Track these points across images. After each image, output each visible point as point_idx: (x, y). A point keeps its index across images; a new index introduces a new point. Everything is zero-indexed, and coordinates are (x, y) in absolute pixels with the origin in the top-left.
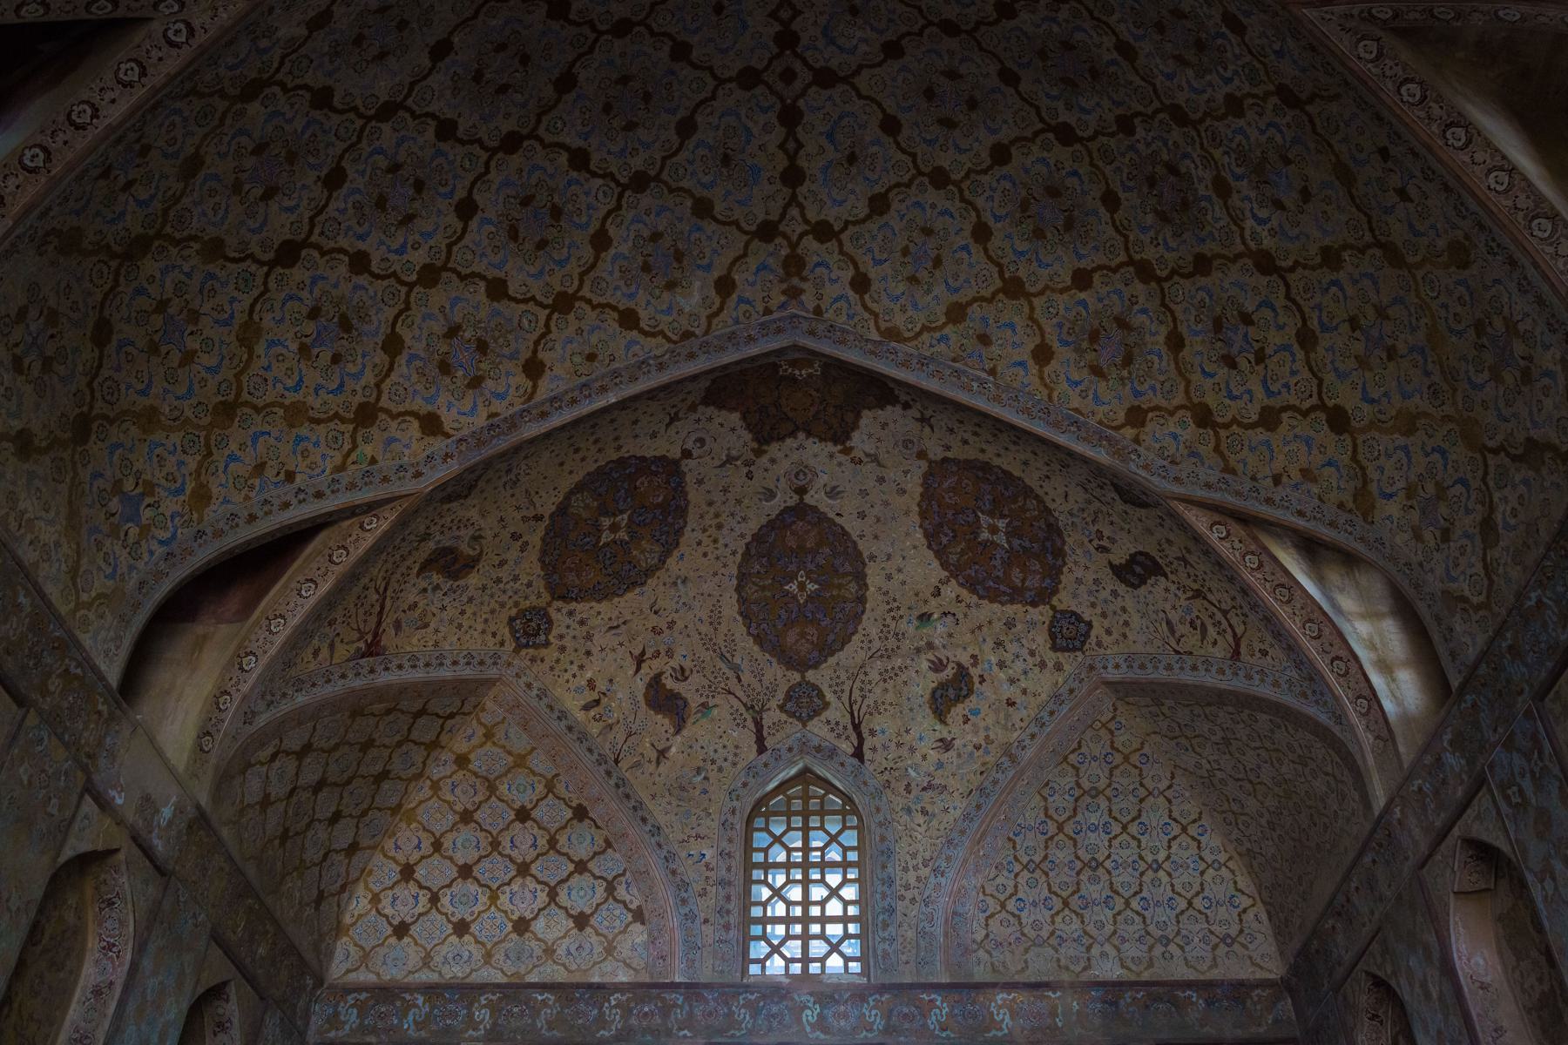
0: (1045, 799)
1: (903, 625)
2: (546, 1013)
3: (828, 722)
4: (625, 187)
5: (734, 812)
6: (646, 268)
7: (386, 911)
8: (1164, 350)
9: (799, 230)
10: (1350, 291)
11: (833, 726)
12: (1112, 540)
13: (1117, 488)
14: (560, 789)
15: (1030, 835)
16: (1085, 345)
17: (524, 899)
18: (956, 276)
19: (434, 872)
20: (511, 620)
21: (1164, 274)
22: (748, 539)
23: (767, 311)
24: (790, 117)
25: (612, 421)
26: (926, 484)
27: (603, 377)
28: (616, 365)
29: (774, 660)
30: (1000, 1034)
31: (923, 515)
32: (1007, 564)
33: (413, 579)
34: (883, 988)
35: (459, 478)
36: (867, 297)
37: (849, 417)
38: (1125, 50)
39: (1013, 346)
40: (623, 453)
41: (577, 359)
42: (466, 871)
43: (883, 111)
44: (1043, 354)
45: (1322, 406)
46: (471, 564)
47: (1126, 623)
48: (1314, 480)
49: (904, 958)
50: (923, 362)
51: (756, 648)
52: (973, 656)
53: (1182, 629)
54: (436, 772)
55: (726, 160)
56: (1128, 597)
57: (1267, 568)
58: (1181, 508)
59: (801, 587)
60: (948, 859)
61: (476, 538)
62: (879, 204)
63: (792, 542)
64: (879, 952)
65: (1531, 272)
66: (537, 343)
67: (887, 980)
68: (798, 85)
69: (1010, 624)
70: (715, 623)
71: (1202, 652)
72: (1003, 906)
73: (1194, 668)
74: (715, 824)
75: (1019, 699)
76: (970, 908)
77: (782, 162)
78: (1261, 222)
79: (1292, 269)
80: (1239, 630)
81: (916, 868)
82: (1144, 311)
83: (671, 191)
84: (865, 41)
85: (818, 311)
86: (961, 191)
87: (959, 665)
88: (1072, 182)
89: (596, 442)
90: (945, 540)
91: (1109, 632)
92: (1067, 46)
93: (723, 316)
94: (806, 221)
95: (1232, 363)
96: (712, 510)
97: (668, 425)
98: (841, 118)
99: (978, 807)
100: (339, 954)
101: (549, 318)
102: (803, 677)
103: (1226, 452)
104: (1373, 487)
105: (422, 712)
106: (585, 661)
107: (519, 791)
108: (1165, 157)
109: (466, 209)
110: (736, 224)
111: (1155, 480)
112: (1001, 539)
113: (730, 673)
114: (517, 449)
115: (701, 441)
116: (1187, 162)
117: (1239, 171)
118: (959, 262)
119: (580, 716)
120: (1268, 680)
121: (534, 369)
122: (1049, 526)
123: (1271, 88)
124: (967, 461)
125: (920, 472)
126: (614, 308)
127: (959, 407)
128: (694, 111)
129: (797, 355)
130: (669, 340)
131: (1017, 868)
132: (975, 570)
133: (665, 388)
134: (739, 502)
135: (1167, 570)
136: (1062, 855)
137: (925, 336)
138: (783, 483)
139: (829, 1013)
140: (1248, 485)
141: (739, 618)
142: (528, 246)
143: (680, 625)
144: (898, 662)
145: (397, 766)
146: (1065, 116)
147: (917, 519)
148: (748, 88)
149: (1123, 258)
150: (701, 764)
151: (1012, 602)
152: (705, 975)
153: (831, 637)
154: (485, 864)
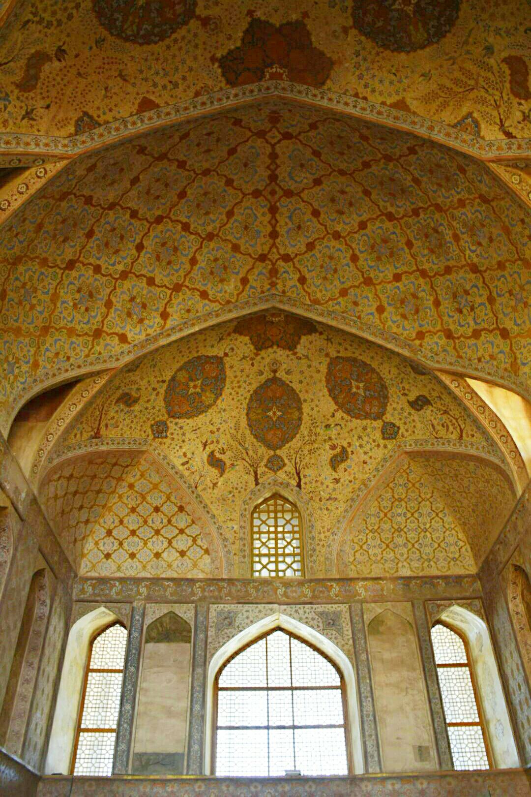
1: (318, 430)
2: (169, 590)
4: (204, 239)
7: (102, 548)
8: (432, 307)
9: (278, 256)
10: (509, 279)
11: (288, 474)
12: (409, 390)
13: (412, 368)
14: (173, 498)
15: (373, 518)
17: (159, 544)
19: (120, 533)
20: (152, 426)
21: (432, 274)
22: (252, 392)
23: (263, 292)
24: (273, 210)
26: (329, 368)
27: (193, 319)
28: (198, 315)
31: (328, 381)
32: (364, 402)
33: (113, 406)
34: (311, 581)
35: (133, 362)
36: (305, 286)
38: (417, 181)
39: (368, 307)
40: (199, 354)
41: (183, 312)
42: (133, 533)
44: (381, 309)
46: (136, 400)
47: (414, 427)
48: (495, 359)
49: (320, 569)
50: (330, 313)
52: (349, 443)
53: (439, 428)
54: (120, 491)
55: (246, 228)
56: (415, 415)
57: (475, 399)
58: (439, 374)
59: (275, 413)
60: (338, 528)
61: (138, 389)
62: (310, 246)
63: (270, 394)
66: (166, 305)
67: (313, 577)
68: (277, 197)
69: (365, 429)
72: (361, 547)
74: (238, 515)
75: (369, 461)
76: (347, 548)
78: (473, 251)
79: (485, 271)
80: (463, 426)
82: (423, 291)
83: (223, 240)
85: (284, 292)
87: (343, 447)
88: (392, 236)
90: (337, 392)
91: (407, 431)
92: (392, 180)
94: (279, 254)
95: (460, 311)
98: (295, 210)
99: (351, 506)
100: (83, 565)
101: (171, 294)
104: (519, 361)
105: (115, 464)
106: (182, 444)
107: (155, 499)
108: (432, 225)
109: (140, 247)
111: (428, 362)
112: (361, 392)
113: (244, 451)
114: (157, 350)
115: (232, 349)
116: (442, 227)
117: (464, 230)
118: (345, 271)
119: (181, 468)
120: (474, 447)
121: (165, 316)
123: (477, 195)
125: (326, 363)
126: (198, 290)
127: (343, 332)
130: (221, 304)
131: (367, 531)
132: (349, 405)
133: (219, 325)
134: (248, 376)
136: (387, 526)
137: (330, 302)
139: (288, 591)
140: (467, 363)
142: (164, 263)
143: (222, 430)
144: (316, 446)
145: (105, 487)
146: (390, 209)
148: (256, 198)
149: (415, 268)
151: (366, 418)
152: (236, 575)
154: (141, 530)
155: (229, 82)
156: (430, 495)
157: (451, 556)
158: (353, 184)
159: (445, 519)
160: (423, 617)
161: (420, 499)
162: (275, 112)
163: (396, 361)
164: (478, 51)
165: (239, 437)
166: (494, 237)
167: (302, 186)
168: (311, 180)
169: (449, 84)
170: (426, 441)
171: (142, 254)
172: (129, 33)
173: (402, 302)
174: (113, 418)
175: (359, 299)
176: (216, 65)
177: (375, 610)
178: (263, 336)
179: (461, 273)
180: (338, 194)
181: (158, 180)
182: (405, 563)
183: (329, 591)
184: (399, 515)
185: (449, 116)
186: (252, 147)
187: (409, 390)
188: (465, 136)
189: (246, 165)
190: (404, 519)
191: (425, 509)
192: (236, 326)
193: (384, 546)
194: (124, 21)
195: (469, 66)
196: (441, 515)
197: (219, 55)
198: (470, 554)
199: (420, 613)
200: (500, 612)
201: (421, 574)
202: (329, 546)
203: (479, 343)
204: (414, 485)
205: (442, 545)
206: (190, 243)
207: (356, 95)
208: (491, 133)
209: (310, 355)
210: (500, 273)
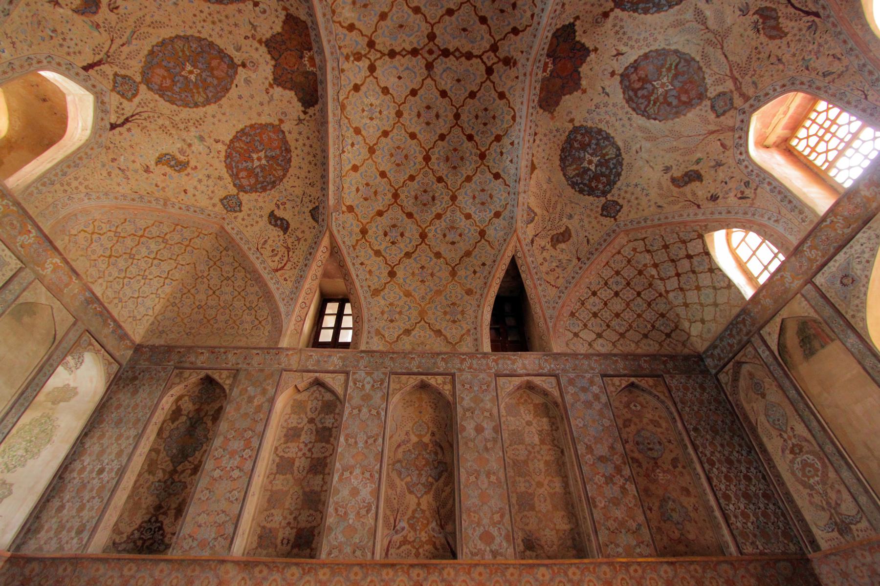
0: (153, 225)
1: (193, 129)
3: (121, 104)
5: (39, 62)
8: (375, 210)
9: (373, 59)
10: (432, 263)
11: (120, 106)
12: (285, 209)
13: (316, 209)
18: (369, 127)
22: (210, 39)
23: (340, 48)
24: (414, 52)
26: (267, 125)
29: (142, 64)
30: (41, 272)
31: (252, 126)
32: (246, 169)
34: (18, 204)
37: (288, 85)
44: (355, 168)
45: (393, 268)
47: (252, 225)
49: (37, 204)
51: (146, 52)
52: (196, 167)
55: (401, 26)
56: (264, 222)
58: (327, 234)
60: (98, 198)
62: (385, 91)
63: (214, 63)
64: (30, 190)
65: (480, 312)
68: (427, 55)
69: (220, 178)
70: (152, 25)
72: (93, 233)
73: (258, 258)
75: (190, 194)
77: (398, 49)
78: (436, 231)
81: (80, 183)
87: (188, 162)
90: (244, 138)
91: (243, 219)
93: (340, 28)
94: (375, 61)
95: (386, 234)
96: (223, 18)
99: (133, 200)
102: (140, 83)
104: (382, 293)
108: (436, 195)
110: (376, 31)
111: (334, 224)
112: (256, 163)
113: (124, 39)
115: (264, 12)
122: (274, 182)
124: (287, 142)
129: (317, 61)
134: (230, 33)
137: (347, 121)
138: (245, 56)
141: (160, 39)
146: (433, 158)
147: (248, 123)
150: (59, 31)
151: (230, 176)
153: (169, 94)
155: (558, 30)
156: (184, 263)
157: (136, 313)
158: (448, 125)
159: (166, 286)
160: (72, 343)
161: (174, 257)
162: (515, 63)
163: (314, 192)
164: (568, 210)
165: (144, 29)
166: (457, 245)
167: (437, 78)
168: (444, 88)
169: (548, 195)
170: (248, 242)
173: (367, 185)
175: (356, 146)
176: (572, 21)
177: (41, 296)
178: (284, 47)
179: (415, 227)
180: (434, 112)
182: (105, 284)
183: (20, 233)
184: (148, 248)
185: (533, 202)
186: (482, 38)
187: (285, 209)
188: (525, 215)
189: (464, 30)
190: (146, 254)
191: (165, 266)
193: (108, 253)
195: (559, 207)
196: (167, 281)
197: (578, 23)
198: (147, 325)
199: (72, 337)
200: (142, 395)
201: (106, 304)
202: (70, 198)
203: (374, 258)
204: (187, 246)
205: (140, 299)
207: (536, 134)
208: (530, 231)
209: (275, 102)
210: (432, 255)
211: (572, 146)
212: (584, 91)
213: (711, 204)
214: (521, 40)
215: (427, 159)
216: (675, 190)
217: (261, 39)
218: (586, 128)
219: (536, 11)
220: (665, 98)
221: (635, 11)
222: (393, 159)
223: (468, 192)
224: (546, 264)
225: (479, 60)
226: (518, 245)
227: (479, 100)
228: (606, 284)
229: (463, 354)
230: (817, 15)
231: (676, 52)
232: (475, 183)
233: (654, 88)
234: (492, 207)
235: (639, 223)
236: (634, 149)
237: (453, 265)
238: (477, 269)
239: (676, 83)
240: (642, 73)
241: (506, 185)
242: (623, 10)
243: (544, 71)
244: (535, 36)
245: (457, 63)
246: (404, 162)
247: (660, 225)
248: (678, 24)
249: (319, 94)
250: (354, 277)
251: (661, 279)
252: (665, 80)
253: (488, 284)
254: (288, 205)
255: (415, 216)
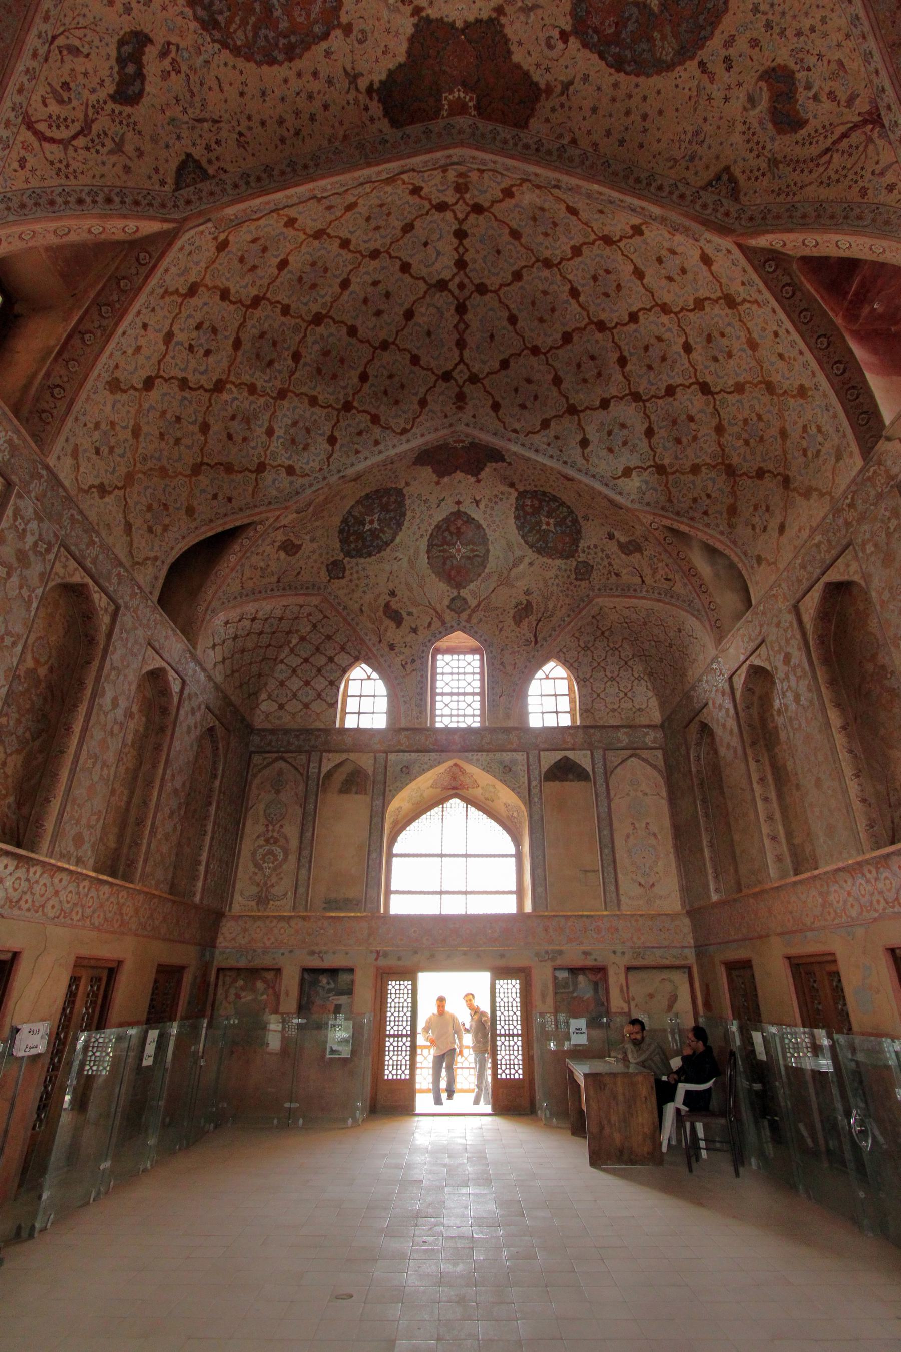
6: (555, 225)
10: (191, 427)
12: (165, 75)
16: (268, 244)
24: (461, 264)
25: (608, 133)
43: (411, 275)
48: (133, 354)
58: (166, 226)
62: (408, 228)
68: (457, 280)
71: (42, 78)
80: (46, 145)
82: (245, 287)
83: (532, 251)
84: (423, 315)
86: (362, 255)
89: (628, 113)
93: (510, 183)
94: (453, 211)
95: (199, 327)
97: (571, 83)
103: (172, 298)
104: (118, 396)
108: (276, 365)
111: (192, 233)
116: (267, 378)
121: (637, 231)
122: (216, 24)
124: (308, 48)
128: (512, 282)
135: (118, 108)
146: (321, 330)
162: (460, 408)
167: (428, 299)
168: (416, 314)
171: (634, 309)
172: (565, 510)
174: (832, 96)
179: (225, 363)
180: (382, 308)
181: (585, 381)
186: (484, 362)
187: (165, 75)
189: (492, 337)
192: (530, 116)
194: (565, 518)
195: (318, 523)
197: (505, 464)
206: (577, 271)
210: (200, 419)
211: (383, 496)
212: (438, 483)
213: (387, 649)
214: (487, 414)
215: (318, 320)
216: (381, 613)
217: (505, 14)
218: (404, 500)
219: (521, 436)
220: (448, 558)
221: (516, 509)
222: (308, 269)
223: (297, 410)
224: (260, 557)
225: (458, 359)
226: (272, 520)
227: (412, 372)
228: (267, 619)
229: (139, 588)
230: (536, 643)
231: (488, 551)
232: (313, 413)
233: (454, 544)
234: (295, 458)
235: (339, 604)
236: (398, 554)
237: (206, 460)
238: (220, 497)
239: (463, 561)
240: (463, 529)
241: (328, 458)
242: (517, 499)
243: (455, 442)
244: (495, 434)
245: (451, 327)
246: (306, 287)
247: (350, 625)
248: (509, 546)
249: (409, 129)
250: (120, 331)
251: (292, 651)
252: (463, 550)
253: (212, 525)
254: (176, 82)
255: (240, 353)
